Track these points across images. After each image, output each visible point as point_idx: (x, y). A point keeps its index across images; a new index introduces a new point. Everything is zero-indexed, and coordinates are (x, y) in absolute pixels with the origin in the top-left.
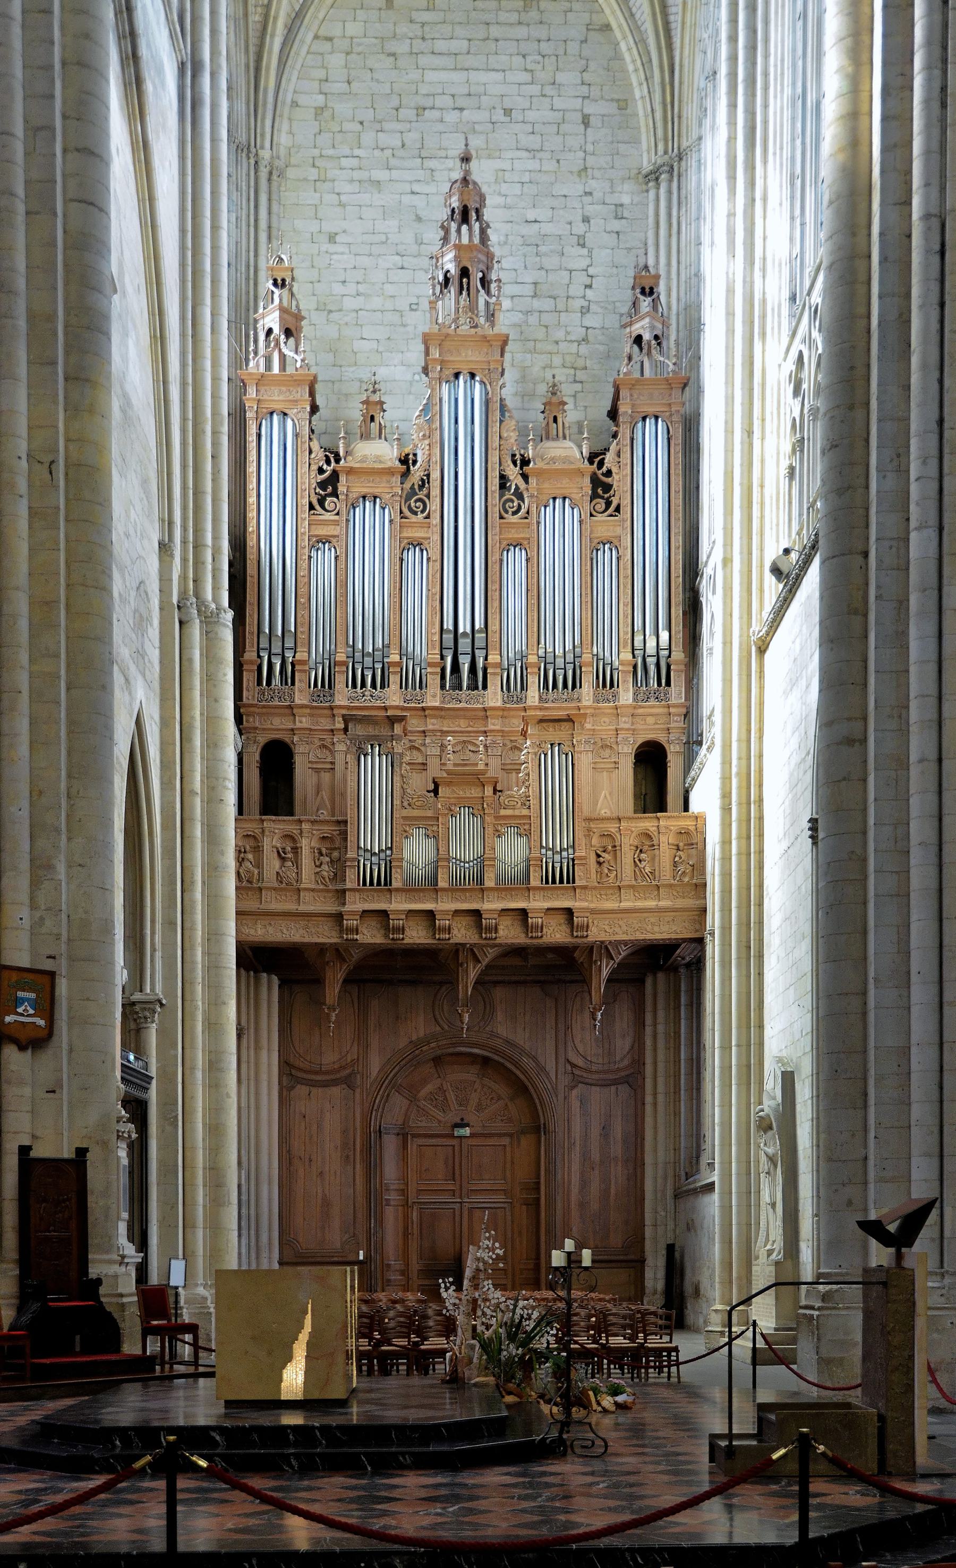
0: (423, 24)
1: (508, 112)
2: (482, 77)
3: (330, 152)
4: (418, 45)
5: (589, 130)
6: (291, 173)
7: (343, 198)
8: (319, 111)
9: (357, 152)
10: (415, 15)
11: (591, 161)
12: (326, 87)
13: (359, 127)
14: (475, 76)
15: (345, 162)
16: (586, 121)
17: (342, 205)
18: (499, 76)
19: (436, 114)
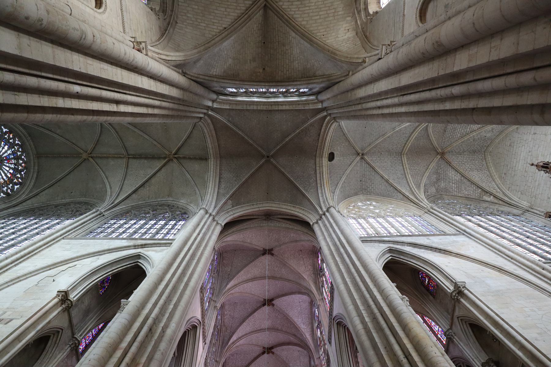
0: (510, 168)
1: (530, 152)
2: (522, 156)
3: (530, 193)
4: (513, 170)
5: (537, 133)
6: (533, 203)
7: (540, 193)
8: (521, 194)
9: (531, 188)
10: (508, 169)
11: (544, 133)
12: (517, 191)
13: (526, 186)
14: (521, 158)
15: (533, 191)
16: (535, 134)
17: (542, 194)
18: (522, 153)
19: (527, 168)
